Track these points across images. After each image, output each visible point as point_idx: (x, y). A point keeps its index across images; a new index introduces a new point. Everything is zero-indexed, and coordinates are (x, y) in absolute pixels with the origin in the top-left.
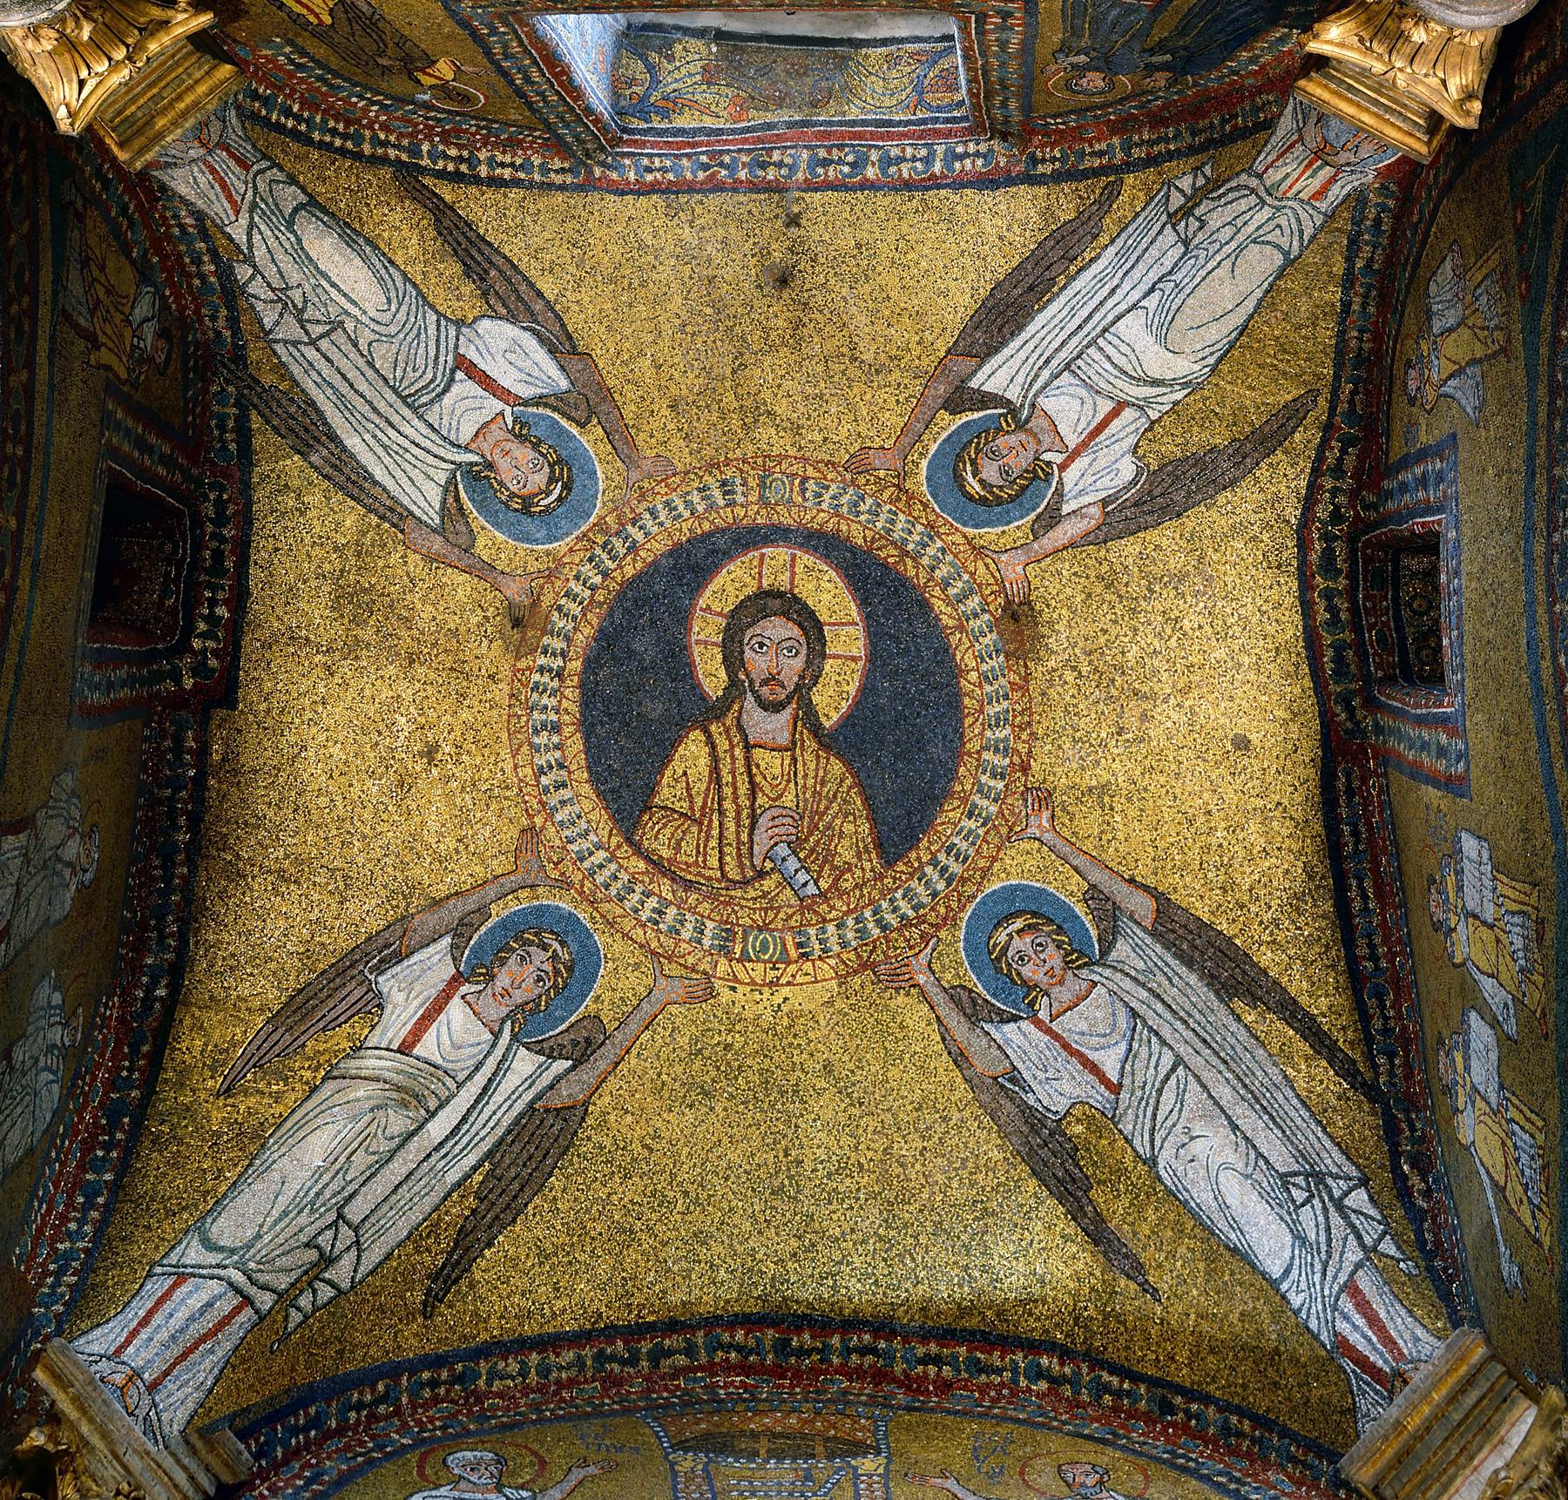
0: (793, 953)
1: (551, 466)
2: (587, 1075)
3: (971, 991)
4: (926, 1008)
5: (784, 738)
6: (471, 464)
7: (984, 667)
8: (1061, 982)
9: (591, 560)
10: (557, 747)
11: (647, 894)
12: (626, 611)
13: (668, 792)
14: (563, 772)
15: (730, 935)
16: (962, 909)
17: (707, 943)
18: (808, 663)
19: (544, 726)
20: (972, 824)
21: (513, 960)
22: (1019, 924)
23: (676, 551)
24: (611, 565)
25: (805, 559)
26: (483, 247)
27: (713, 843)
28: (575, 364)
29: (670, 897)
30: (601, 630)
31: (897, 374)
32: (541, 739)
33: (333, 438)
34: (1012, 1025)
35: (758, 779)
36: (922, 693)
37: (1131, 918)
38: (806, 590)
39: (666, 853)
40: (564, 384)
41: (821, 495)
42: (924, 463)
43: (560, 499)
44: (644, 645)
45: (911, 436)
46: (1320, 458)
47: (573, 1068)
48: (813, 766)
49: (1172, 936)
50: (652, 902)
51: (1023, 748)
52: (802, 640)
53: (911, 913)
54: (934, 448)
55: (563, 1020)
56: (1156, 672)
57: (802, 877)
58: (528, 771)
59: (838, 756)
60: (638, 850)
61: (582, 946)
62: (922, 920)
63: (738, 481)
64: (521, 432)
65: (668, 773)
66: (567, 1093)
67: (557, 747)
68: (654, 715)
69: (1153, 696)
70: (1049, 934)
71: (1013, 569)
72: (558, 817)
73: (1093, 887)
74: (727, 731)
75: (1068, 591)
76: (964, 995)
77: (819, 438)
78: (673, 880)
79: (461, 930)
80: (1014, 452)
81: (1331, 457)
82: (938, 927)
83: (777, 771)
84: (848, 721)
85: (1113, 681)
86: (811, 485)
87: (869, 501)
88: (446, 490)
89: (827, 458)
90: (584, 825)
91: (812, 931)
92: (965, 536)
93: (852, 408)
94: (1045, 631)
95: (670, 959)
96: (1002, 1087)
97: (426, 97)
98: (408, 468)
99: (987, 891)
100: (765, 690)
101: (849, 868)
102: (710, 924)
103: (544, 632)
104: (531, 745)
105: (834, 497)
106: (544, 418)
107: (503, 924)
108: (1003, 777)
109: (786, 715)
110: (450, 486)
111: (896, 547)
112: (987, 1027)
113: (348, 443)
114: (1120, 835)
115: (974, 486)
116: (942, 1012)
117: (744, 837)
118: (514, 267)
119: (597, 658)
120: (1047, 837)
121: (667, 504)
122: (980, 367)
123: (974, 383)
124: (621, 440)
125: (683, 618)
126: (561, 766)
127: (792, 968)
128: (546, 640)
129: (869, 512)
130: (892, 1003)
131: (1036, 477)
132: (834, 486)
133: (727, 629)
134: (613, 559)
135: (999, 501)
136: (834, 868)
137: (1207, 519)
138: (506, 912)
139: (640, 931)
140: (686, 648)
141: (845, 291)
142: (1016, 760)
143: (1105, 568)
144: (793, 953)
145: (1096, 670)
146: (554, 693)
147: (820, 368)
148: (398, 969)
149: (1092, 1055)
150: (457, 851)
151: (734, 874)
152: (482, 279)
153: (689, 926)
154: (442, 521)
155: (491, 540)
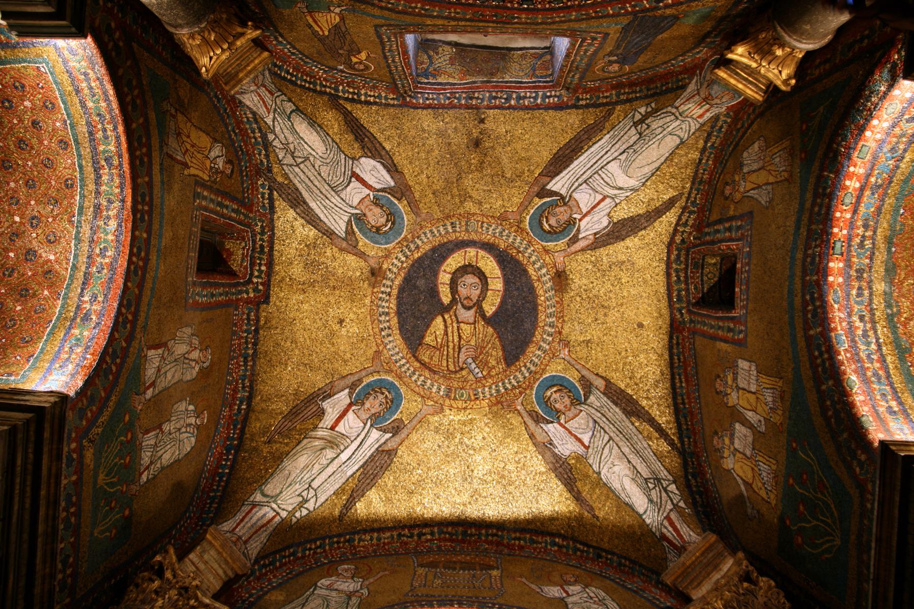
0: (473, 398)
1: (387, 215)
2: (397, 439)
3: (536, 412)
4: (520, 418)
5: (471, 320)
6: (357, 214)
7: (547, 295)
8: (569, 410)
9: (401, 252)
10: (388, 321)
11: (420, 375)
12: (415, 272)
13: (428, 339)
14: (390, 331)
15: (449, 390)
16: (535, 383)
17: (442, 393)
18: (482, 292)
19: (383, 313)
20: (539, 353)
21: (371, 398)
22: (555, 389)
23: (434, 250)
24: (409, 253)
25: (482, 253)
26: (363, 129)
27: (445, 357)
28: (397, 176)
29: (428, 376)
30: (405, 278)
31: (519, 183)
32: (383, 318)
33: (305, 202)
34: (551, 425)
35: (462, 334)
36: (523, 304)
37: (596, 388)
38: (481, 264)
39: (427, 360)
40: (393, 184)
41: (488, 229)
42: (528, 217)
43: (390, 228)
44: (421, 283)
45: (523, 207)
46: (680, 219)
47: (393, 436)
48: (482, 330)
49: (610, 395)
50: (422, 378)
51: (560, 325)
52: (480, 283)
53: (516, 384)
54: (532, 211)
55: (389, 419)
56: (610, 298)
57: (477, 370)
58: (377, 330)
59: (492, 327)
60: (417, 360)
61: (396, 393)
62: (520, 386)
63: (458, 223)
64: (376, 202)
65: (429, 331)
66: (390, 446)
67: (388, 321)
68: (424, 310)
69: (608, 308)
70: (566, 393)
71: (559, 258)
72: (388, 347)
73: (583, 376)
74: (451, 316)
75: (580, 267)
76: (534, 414)
77: (489, 207)
78: (430, 370)
79: (352, 387)
80: (562, 213)
81: (684, 219)
82: (525, 389)
83: (469, 332)
84: (496, 314)
85: (594, 301)
86: (485, 225)
87: (507, 231)
88: (347, 224)
89: (491, 214)
90: (397, 350)
91: (480, 390)
92: (542, 245)
93: (501, 195)
94: (570, 282)
95: (428, 399)
96: (546, 446)
97: (342, 67)
98: (333, 215)
99: (544, 377)
100: (465, 302)
101: (494, 367)
102: (443, 387)
103: (384, 278)
104: (379, 320)
105: (493, 230)
106: (385, 197)
107: (368, 385)
108: (552, 335)
109: (472, 312)
110: (349, 223)
111: (516, 249)
112: (542, 425)
113: (311, 205)
114: (594, 358)
115: (546, 227)
116: (526, 419)
117: (456, 356)
118: (374, 137)
119: (404, 287)
120: (567, 358)
121: (431, 231)
122: (551, 181)
123: (548, 187)
124: (414, 206)
125: (436, 274)
126: (389, 328)
127: (472, 403)
128: (384, 281)
129: (507, 236)
130: (508, 416)
131: (570, 224)
132: (493, 226)
133: (452, 279)
134: (410, 251)
135: (555, 232)
136: (489, 367)
137: (632, 242)
138: (368, 381)
139: (417, 388)
140: (436, 285)
141: (500, 150)
142: (557, 329)
143: (593, 259)
144: (473, 398)
145: (588, 297)
146: (387, 301)
147: (490, 180)
148: (329, 400)
149: (579, 436)
150: (351, 358)
151: (452, 368)
152: (362, 142)
153: (435, 387)
154: (346, 234)
155: (363, 242)
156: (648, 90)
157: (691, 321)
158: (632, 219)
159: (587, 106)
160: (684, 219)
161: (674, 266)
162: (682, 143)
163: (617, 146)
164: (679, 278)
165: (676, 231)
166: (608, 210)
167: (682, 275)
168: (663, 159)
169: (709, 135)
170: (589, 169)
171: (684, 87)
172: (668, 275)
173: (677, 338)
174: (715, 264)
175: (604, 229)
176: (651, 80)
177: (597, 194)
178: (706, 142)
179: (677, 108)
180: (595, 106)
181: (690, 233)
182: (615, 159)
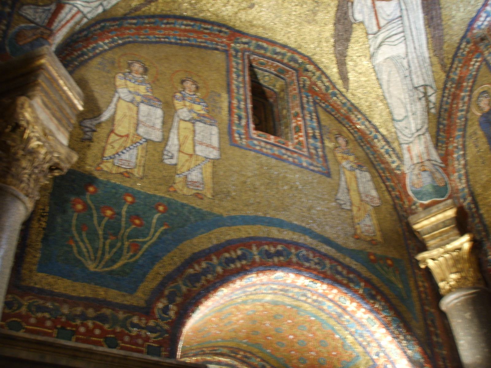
81: (325, 80)
137: (329, 30)
156: (446, 110)
157: (237, 51)
158: (348, 40)
159: (459, 48)
160: (325, 80)
161: (289, 54)
162: (393, 120)
163: (416, 61)
164: (277, 53)
165: (319, 69)
166: (367, 23)
167: (279, 58)
168: (387, 95)
169: (388, 143)
170: (410, 26)
171: (436, 146)
172: (284, 46)
173: (225, 33)
174: (274, 86)
175: (353, 13)
176: (450, 116)
177: (385, 22)
178: (383, 136)
179: (423, 134)
180: (455, 55)
181: (310, 78)
182: (407, 55)
